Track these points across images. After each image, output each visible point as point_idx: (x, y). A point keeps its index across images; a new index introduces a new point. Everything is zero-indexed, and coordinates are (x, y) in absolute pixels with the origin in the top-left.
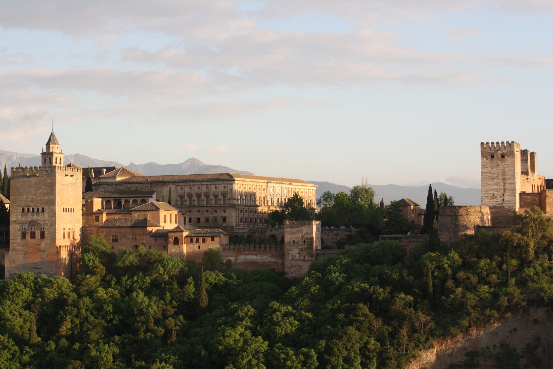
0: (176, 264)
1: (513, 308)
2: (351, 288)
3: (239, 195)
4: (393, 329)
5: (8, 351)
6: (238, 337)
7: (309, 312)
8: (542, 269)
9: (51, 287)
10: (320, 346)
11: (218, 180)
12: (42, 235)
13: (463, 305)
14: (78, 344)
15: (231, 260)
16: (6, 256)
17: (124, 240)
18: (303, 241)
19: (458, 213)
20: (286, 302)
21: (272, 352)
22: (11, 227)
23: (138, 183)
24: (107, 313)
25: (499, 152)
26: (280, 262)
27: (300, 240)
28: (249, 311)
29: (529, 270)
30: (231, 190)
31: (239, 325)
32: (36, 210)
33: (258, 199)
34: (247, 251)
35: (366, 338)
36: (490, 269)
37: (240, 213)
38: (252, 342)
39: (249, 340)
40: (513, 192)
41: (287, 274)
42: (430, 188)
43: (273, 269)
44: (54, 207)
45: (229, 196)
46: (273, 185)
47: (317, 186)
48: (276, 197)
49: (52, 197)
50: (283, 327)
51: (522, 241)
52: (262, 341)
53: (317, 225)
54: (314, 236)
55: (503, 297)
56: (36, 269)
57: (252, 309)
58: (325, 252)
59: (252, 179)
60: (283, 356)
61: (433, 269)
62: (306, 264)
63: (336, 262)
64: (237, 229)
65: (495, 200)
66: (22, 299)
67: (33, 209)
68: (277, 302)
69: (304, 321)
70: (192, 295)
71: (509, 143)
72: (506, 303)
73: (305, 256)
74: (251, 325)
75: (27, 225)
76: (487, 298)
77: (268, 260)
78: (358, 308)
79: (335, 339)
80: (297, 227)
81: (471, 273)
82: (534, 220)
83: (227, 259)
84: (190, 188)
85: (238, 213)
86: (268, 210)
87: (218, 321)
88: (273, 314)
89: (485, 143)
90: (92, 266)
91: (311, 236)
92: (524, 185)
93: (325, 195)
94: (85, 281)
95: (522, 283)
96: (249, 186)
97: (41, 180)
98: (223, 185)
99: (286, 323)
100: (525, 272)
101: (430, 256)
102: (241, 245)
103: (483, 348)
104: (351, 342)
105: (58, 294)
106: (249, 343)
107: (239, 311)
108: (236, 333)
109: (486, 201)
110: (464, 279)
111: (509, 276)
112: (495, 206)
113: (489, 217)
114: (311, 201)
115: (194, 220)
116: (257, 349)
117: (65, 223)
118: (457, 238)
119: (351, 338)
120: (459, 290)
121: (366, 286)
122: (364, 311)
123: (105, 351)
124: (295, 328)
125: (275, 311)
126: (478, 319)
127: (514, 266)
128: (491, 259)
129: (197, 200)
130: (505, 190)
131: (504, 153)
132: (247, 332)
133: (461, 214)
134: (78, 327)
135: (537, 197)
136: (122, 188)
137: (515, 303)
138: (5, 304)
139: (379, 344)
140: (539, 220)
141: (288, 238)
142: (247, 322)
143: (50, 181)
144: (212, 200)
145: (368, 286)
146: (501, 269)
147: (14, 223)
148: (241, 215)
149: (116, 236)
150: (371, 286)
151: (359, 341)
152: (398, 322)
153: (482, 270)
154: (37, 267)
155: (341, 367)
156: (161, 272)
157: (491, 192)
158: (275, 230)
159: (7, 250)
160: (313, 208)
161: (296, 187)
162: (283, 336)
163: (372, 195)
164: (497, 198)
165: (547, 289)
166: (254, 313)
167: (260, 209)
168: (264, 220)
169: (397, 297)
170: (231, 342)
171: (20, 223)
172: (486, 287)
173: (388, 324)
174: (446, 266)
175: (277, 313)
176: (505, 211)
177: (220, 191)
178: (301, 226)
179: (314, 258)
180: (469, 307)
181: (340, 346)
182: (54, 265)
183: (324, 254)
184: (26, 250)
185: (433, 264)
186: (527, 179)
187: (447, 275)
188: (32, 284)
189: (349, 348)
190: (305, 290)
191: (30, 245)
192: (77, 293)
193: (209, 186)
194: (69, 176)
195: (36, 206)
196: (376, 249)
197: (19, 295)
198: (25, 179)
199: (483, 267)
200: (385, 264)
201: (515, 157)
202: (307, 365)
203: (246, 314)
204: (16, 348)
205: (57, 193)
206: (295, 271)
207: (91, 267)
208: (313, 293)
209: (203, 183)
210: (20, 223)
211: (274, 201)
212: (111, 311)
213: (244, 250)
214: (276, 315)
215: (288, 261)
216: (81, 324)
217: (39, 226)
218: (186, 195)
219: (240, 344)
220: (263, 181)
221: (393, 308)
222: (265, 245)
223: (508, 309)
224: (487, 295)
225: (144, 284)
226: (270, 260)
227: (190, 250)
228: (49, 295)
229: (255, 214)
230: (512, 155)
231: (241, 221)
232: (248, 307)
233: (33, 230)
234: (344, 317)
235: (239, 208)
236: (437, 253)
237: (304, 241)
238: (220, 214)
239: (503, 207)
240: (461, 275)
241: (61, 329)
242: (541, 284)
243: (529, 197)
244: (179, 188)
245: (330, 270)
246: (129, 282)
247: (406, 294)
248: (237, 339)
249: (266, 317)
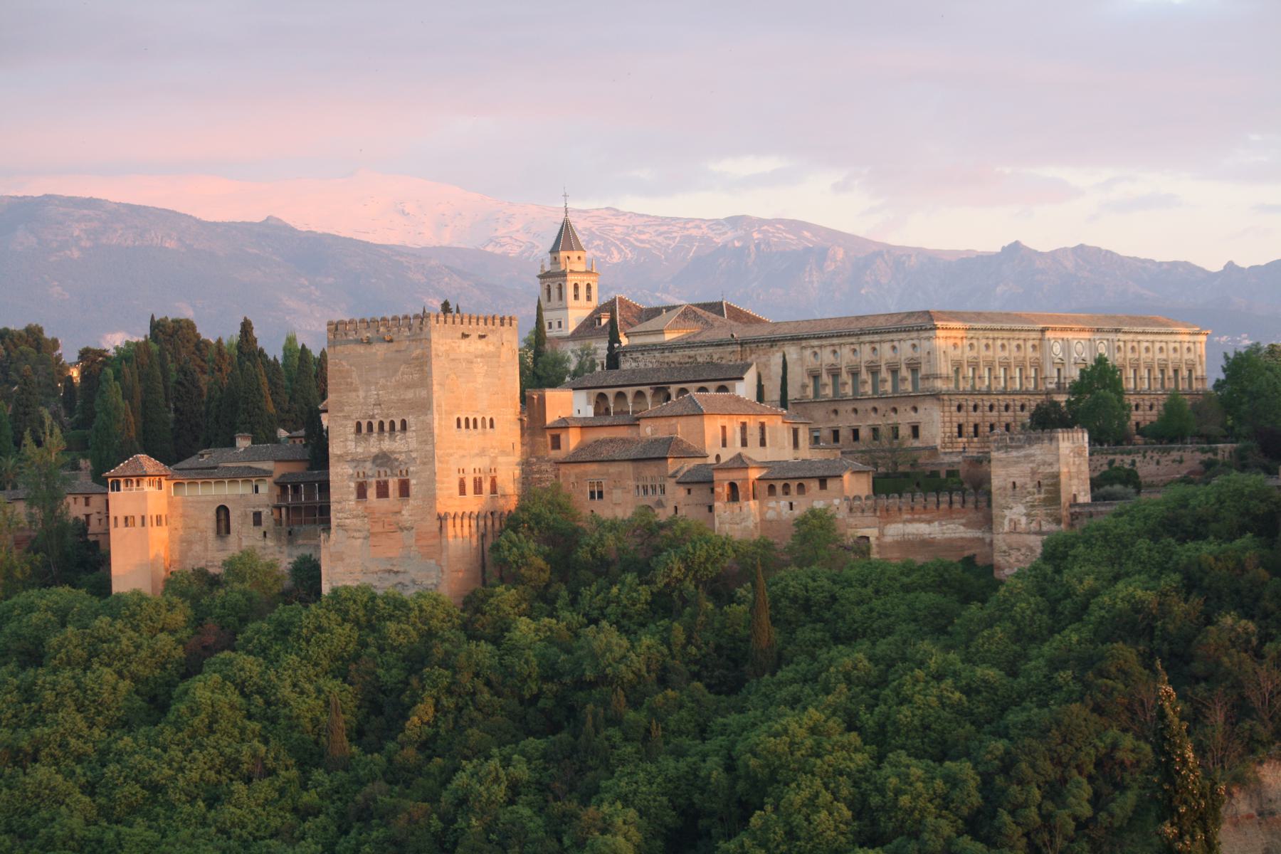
0: (720, 551)
3: (953, 366)
5: (272, 783)
6: (801, 733)
9: (403, 618)
10: (989, 756)
12: (404, 490)
14: (438, 760)
16: (322, 544)
17: (617, 495)
18: (1036, 483)
22: (331, 470)
23: (712, 345)
24: (524, 681)
27: (1028, 480)
28: (855, 667)
30: (929, 353)
32: (387, 427)
35: (1114, 732)
37: (954, 414)
38: (833, 748)
41: (1000, 568)
44: (429, 416)
45: (924, 370)
46: (1059, 335)
49: (424, 393)
56: (392, 574)
60: (894, 781)
64: (945, 453)
66: (330, 651)
67: (381, 424)
70: (741, 629)
73: (1043, 523)
75: (369, 465)
77: (957, 535)
84: (835, 352)
85: (947, 414)
90: (516, 562)
91: (1055, 469)
94: (491, 600)
97: (397, 351)
98: (911, 342)
102: (893, 497)
105: (421, 636)
115: (845, 434)
117: (464, 456)
119: (1072, 734)
122: (1122, 662)
123: (490, 778)
129: (850, 382)
134: (450, 716)
136: (676, 359)
138: (284, 664)
141: (1000, 477)
143: (418, 351)
144: (885, 381)
147: (338, 461)
148: (961, 417)
149: (599, 484)
154: (395, 569)
155: (1034, 809)
156: (675, 573)
159: (324, 530)
161: (1140, 337)
171: (353, 460)
177: (903, 358)
178: (1029, 444)
179: (1063, 526)
182: (433, 562)
183: (1091, 515)
184: (367, 526)
188: (360, 613)
191: (377, 515)
192: (469, 632)
193: (877, 346)
194: (474, 336)
195: (387, 416)
197: (324, 641)
198: (361, 349)
200: (1211, 538)
202: (952, 806)
204: (294, 773)
205: (435, 382)
206: (1018, 561)
207: (515, 566)
209: (864, 338)
210: (353, 460)
212: (534, 675)
213: (900, 509)
215: (1000, 537)
216: (460, 710)
217: (397, 467)
218: (824, 371)
225: (634, 605)
226: (964, 535)
227: (771, 515)
228: (395, 640)
233: (383, 478)
238: (905, 418)
241: (408, 724)
244: (808, 353)
246: (598, 601)
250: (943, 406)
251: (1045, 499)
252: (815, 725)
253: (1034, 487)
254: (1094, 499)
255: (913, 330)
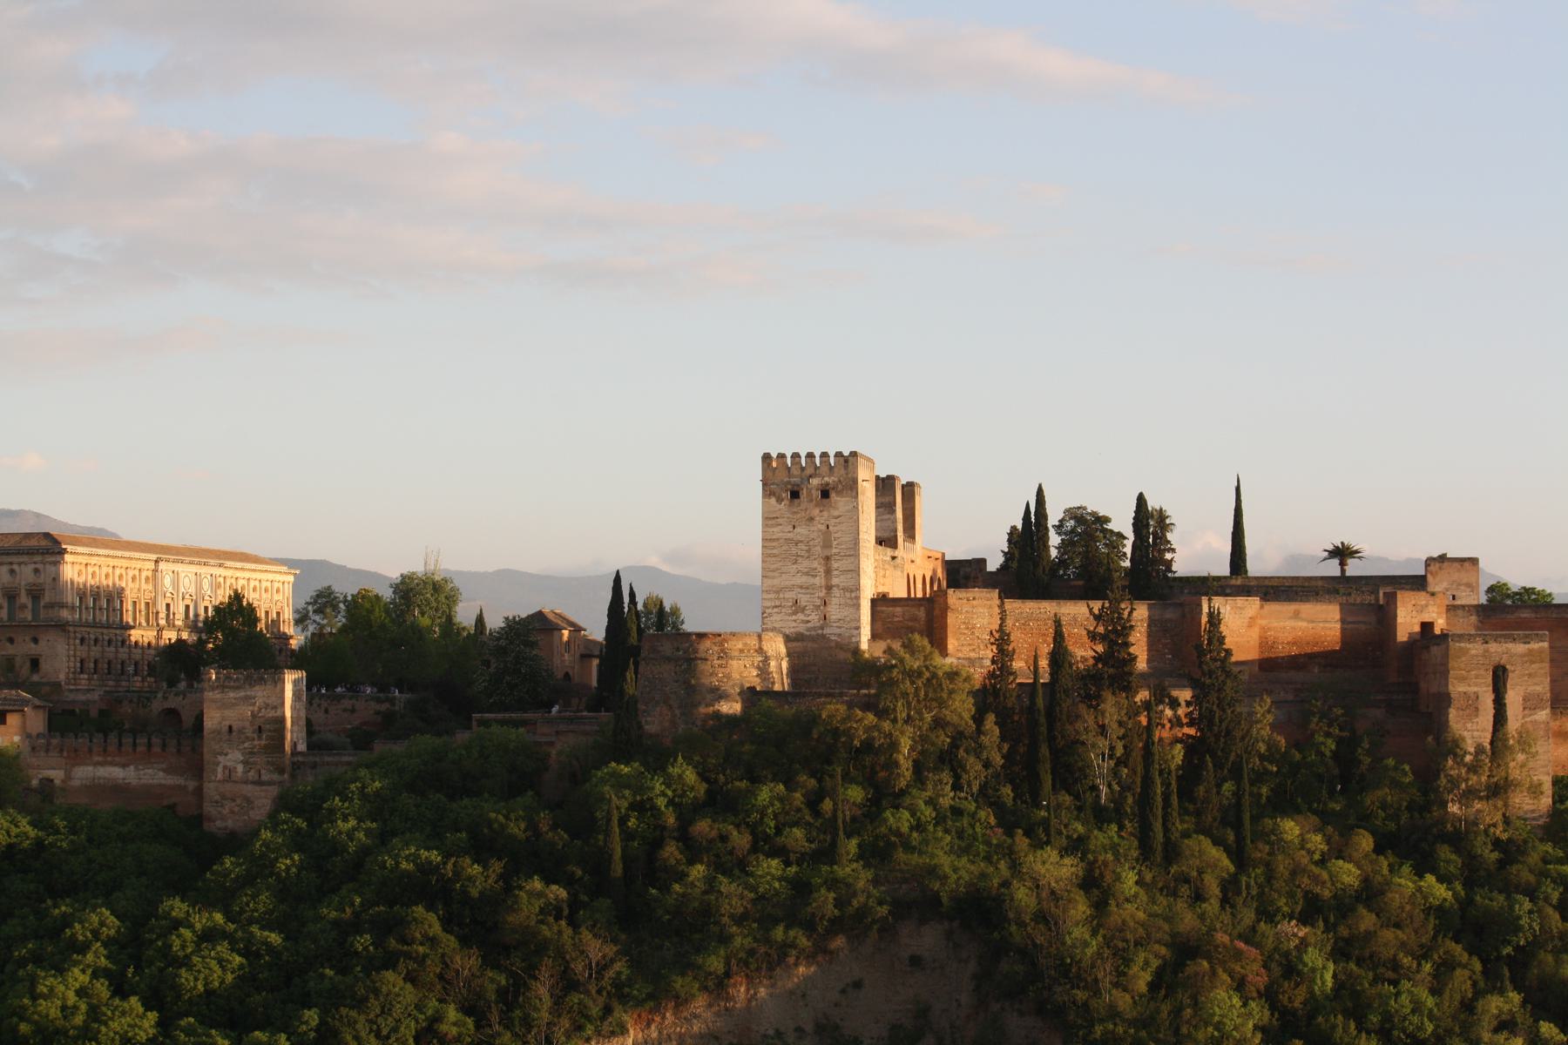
1: (852, 922)
2: (390, 862)
3: (78, 594)
4: (511, 981)
6: (72, 998)
7: (272, 930)
8: (934, 815)
11: (19, 552)
13: (707, 913)
15: (52, 781)
19: (697, 652)
20: (209, 904)
21: (168, 1041)
25: (815, 482)
26: (191, 788)
27: (247, 724)
28: (102, 924)
29: (897, 816)
30: (54, 579)
31: (76, 963)
33: (130, 608)
34: (99, 755)
35: (433, 1004)
36: (787, 813)
37: (79, 647)
38: (113, 1014)
39: (104, 1009)
40: (853, 595)
42: (617, 580)
43: (172, 807)
45: (47, 598)
46: (171, 566)
47: (298, 572)
48: (181, 602)
50: (199, 971)
51: (876, 734)
52: (141, 1010)
53: (295, 683)
54: (288, 714)
55: (823, 891)
57: (112, 920)
58: (317, 759)
59: (113, 548)
61: (623, 811)
62: (263, 794)
63: (349, 788)
64: (71, 691)
65: (800, 616)
68: (183, 901)
69: (258, 955)
71: (843, 456)
72: (830, 910)
73: (263, 772)
74: (110, 966)
76: (777, 893)
77: (155, 781)
78: (410, 918)
79: (345, 1006)
80: (238, 688)
81: (732, 824)
82: (913, 675)
83: (41, 776)
85: (72, 647)
86: (159, 637)
87: (17, 954)
88: (172, 934)
89: (774, 455)
91: (279, 713)
92: (884, 576)
93: (318, 596)
95: (877, 853)
96: (105, 570)
98: (33, 566)
99: (208, 960)
100: (886, 820)
101: (614, 774)
103: (765, 1036)
104: (391, 1015)
106: (105, 1015)
107: (76, 924)
108: (67, 988)
109: (776, 619)
110: (711, 841)
111: (841, 833)
112: (802, 634)
113: (785, 665)
114: (278, 614)
116: (127, 1032)
118: (693, 724)
120: (698, 871)
121: (435, 856)
122: (426, 927)
124: (232, 973)
125: (177, 924)
126: (751, 952)
127: (854, 802)
128: (790, 784)
130: (829, 588)
131: (828, 484)
132: (99, 985)
133: (703, 656)
135: (922, 608)
137: (857, 909)
139: (470, 1022)
140: (927, 675)
141: (212, 720)
142: (97, 956)
145: (439, 858)
146: (817, 813)
148: (82, 651)
150: (447, 856)
151: (415, 1012)
152: (523, 961)
153: (763, 814)
157: (790, 595)
158: (177, 694)
160: (285, 634)
161: (239, 574)
162: (200, 996)
163: (452, 599)
164: (807, 612)
165: (947, 870)
166: (118, 932)
167: (135, 635)
168: (146, 668)
169: (521, 888)
170: (52, 1011)
172: (774, 862)
173: (497, 967)
174: (661, 802)
175: (182, 930)
176: (831, 648)
177: (23, 583)
178: (250, 684)
179: (286, 776)
180: (725, 920)
181: (359, 1026)
183: (314, 766)
185: (624, 797)
186: (894, 558)
187: (664, 828)
189: (385, 1032)
190: (260, 868)
196: (464, 752)
199: (765, 808)
200: (486, 795)
201: (860, 497)
203: (96, 934)
206: (232, 812)
208: (284, 874)
211: (174, 614)
213: (90, 751)
214: (179, 936)
215: (211, 785)
219: (79, 1019)
220: (143, 556)
221: (510, 919)
222: (149, 740)
223: (836, 926)
224: (777, 885)
226: (163, 782)
229: (121, 650)
230: (851, 489)
231: (81, 668)
232: (101, 913)
234: (372, 944)
235: (75, 632)
236: (636, 765)
237: (260, 727)
238: (23, 648)
239: (823, 636)
240: (703, 827)
242: (932, 856)
243: (899, 609)
245: (332, 811)
247: (548, 881)
248: (70, 1003)
249: (152, 942)
250: (69, 638)
251: (266, 747)
252: (81, 987)
253: (253, 733)
254: (309, 747)
255: (38, 553)
